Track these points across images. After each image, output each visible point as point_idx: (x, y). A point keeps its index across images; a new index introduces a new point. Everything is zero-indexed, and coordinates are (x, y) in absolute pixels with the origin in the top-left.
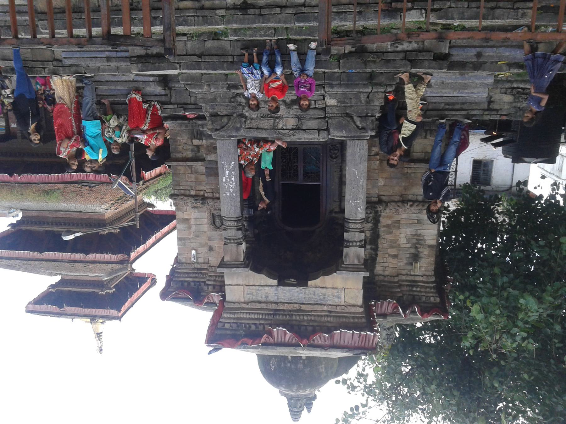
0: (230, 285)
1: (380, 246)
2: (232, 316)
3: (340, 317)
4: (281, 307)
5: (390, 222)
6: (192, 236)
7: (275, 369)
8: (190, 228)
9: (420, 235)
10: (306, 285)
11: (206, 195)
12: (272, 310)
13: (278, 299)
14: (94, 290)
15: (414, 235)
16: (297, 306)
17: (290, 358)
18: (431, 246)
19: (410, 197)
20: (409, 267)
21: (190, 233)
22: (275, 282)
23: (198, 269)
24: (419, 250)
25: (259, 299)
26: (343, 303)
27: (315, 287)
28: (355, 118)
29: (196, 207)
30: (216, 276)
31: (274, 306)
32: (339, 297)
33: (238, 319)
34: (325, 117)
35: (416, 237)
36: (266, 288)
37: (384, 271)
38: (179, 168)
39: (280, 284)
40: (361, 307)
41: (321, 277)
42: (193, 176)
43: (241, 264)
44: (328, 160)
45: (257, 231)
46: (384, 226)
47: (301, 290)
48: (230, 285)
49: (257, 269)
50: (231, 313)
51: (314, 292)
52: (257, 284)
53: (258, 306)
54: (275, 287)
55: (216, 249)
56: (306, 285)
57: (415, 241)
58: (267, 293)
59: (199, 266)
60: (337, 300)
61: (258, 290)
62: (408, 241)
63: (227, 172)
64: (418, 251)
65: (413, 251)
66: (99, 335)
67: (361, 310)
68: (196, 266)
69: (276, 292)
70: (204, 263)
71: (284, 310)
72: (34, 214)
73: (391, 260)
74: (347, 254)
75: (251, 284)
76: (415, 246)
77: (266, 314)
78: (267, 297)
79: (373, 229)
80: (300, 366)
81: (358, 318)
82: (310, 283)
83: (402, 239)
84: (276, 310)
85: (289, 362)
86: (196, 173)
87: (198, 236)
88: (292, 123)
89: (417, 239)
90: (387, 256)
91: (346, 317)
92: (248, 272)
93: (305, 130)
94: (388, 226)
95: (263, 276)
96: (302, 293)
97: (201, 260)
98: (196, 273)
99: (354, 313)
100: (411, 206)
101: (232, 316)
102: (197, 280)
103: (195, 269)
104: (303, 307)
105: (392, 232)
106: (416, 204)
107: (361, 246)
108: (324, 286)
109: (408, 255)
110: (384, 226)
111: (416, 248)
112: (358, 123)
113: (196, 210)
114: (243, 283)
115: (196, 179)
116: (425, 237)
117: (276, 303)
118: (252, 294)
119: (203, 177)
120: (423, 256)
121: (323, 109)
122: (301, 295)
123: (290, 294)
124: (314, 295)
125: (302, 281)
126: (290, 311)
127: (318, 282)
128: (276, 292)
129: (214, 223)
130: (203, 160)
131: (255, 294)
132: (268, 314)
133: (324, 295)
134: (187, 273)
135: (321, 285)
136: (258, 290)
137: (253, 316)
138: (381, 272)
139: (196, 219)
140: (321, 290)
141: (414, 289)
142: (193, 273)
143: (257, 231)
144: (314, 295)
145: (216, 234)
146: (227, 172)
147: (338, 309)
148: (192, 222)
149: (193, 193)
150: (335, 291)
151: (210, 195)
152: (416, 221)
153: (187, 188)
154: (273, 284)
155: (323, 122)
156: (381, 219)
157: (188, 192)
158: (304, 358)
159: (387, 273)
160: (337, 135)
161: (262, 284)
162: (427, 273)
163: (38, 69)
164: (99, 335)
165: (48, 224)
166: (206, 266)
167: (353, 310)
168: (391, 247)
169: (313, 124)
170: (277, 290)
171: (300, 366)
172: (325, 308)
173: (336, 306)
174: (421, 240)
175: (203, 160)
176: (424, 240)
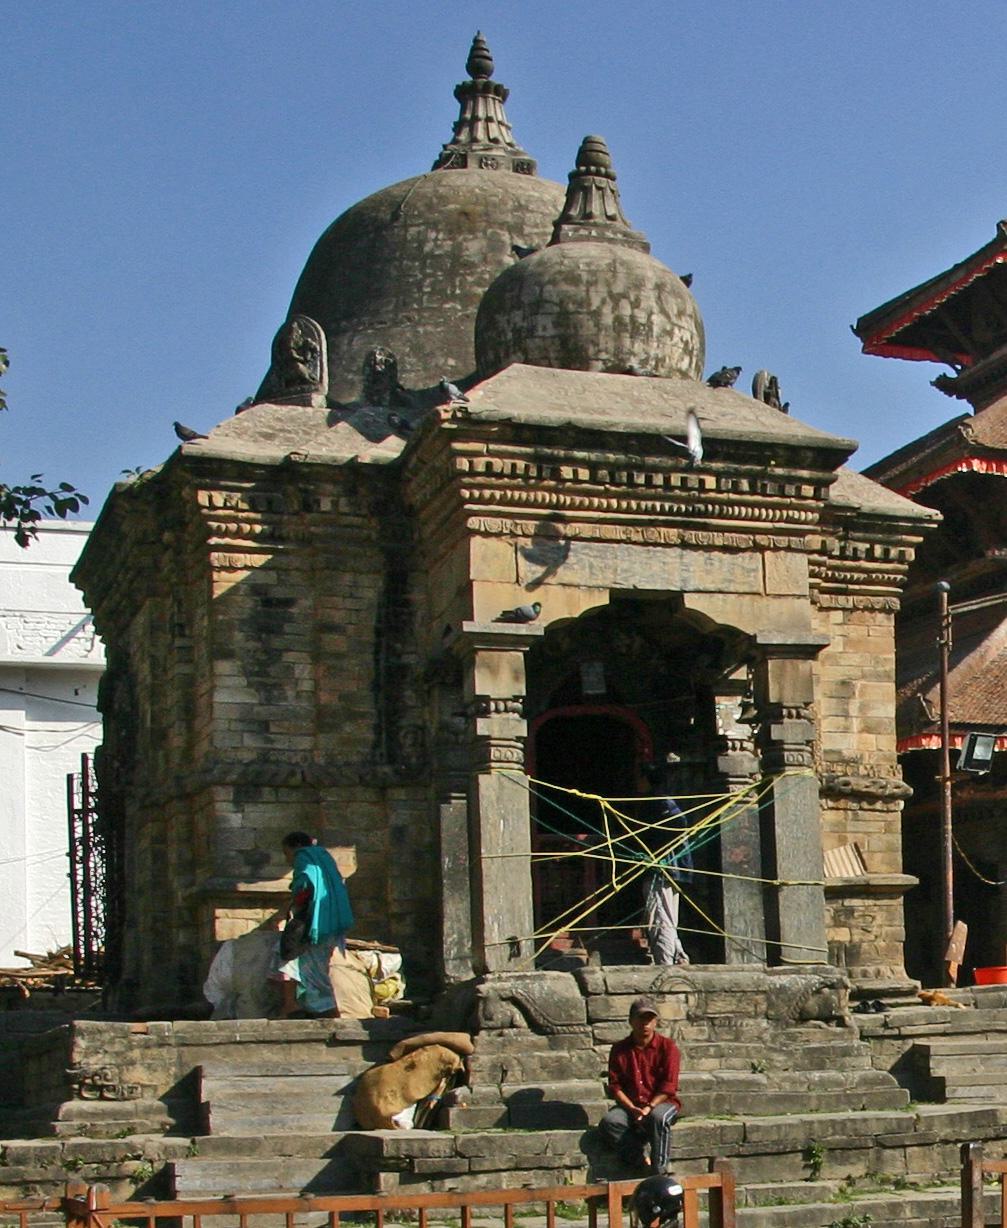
0: (799, 597)
1: (369, 657)
5: (348, 728)
10: (615, 594)
13: (681, 557)
19: (294, 796)
22: (691, 602)
24: (258, 645)
31: (692, 536)
35: (271, 681)
36: (712, 587)
39: (676, 597)
41: (576, 615)
43: (773, 653)
46: (363, 716)
47: (626, 579)
48: (799, 597)
50: (797, 522)
51: (592, 573)
52: (733, 596)
54: (691, 588)
57: (273, 670)
58: (708, 572)
61: (730, 581)
62: (289, 668)
64: (259, 639)
65: (277, 643)
67: (473, 523)
69: (685, 575)
73: (338, 617)
74: (516, 678)
75: (748, 597)
76: (273, 655)
77: (712, 516)
81: (481, 501)
83: (306, 675)
89: (268, 676)
90: (351, 629)
94: (352, 716)
95: (719, 620)
96: (626, 571)
105: (340, 698)
108: (568, 590)
109: (287, 628)
110: (363, 716)
114: (765, 601)
116: (243, 681)
122: (625, 565)
124: (591, 566)
128: (685, 575)
131: (738, 571)
136: (730, 581)
140: (576, 580)
144: (591, 566)
152: (273, 729)
154: (696, 596)
156: (370, 736)
159: (348, 578)
161: (721, 596)
167: (494, 524)
168: (339, 656)
170: (684, 580)
174: (258, 674)
176: (247, 673)
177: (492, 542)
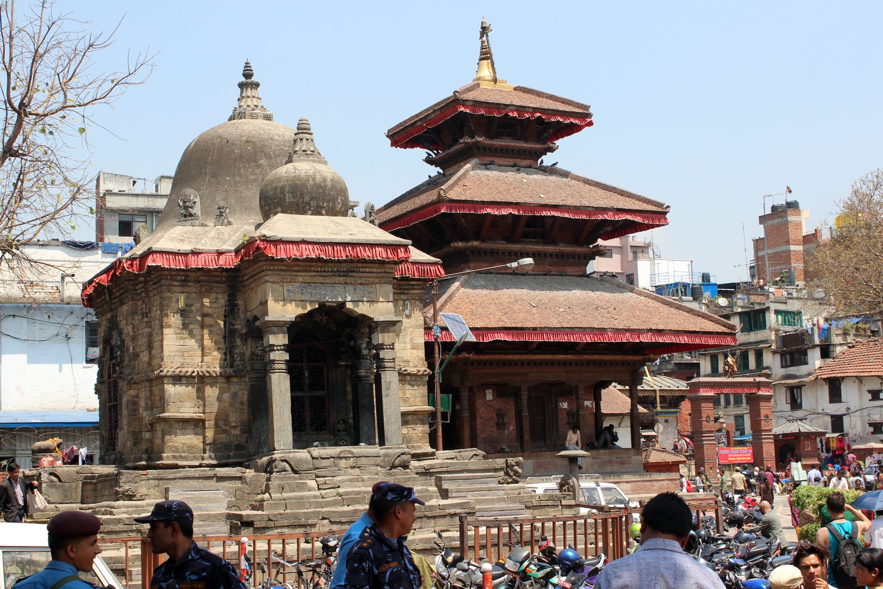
8: (412, 339)
14: (491, 142)
16: (328, 281)
17: (324, 212)
18: (169, 326)
20: (190, 302)
23: (403, 294)
25: (361, 287)
26: (285, 284)
31: (348, 280)
32: (288, 290)
37: (217, 298)
45: (352, 343)
53: (363, 280)
59: (402, 297)
60: (291, 288)
66: (486, 55)
71: (339, 276)
72: (569, 270)
78: (355, 290)
79: (233, 347)
80: (313, 203)
84: (346, 276)
100: (193, 372)
106: (188, 374)
107: (273, 345)
117: (346, 283)
118: (369, 292)
121: (317, 476)
123: (333, 295)
133: (302, 293)
137: (368, 270)
138: (220, 296)
140: (306, 299)
143: (352, 343)
148: (409, 346)
150: (292, 298)
158: (310, 212)
162: (169, 294)
164: (486, 55)
165: (551, 255)
167: (275, 279)
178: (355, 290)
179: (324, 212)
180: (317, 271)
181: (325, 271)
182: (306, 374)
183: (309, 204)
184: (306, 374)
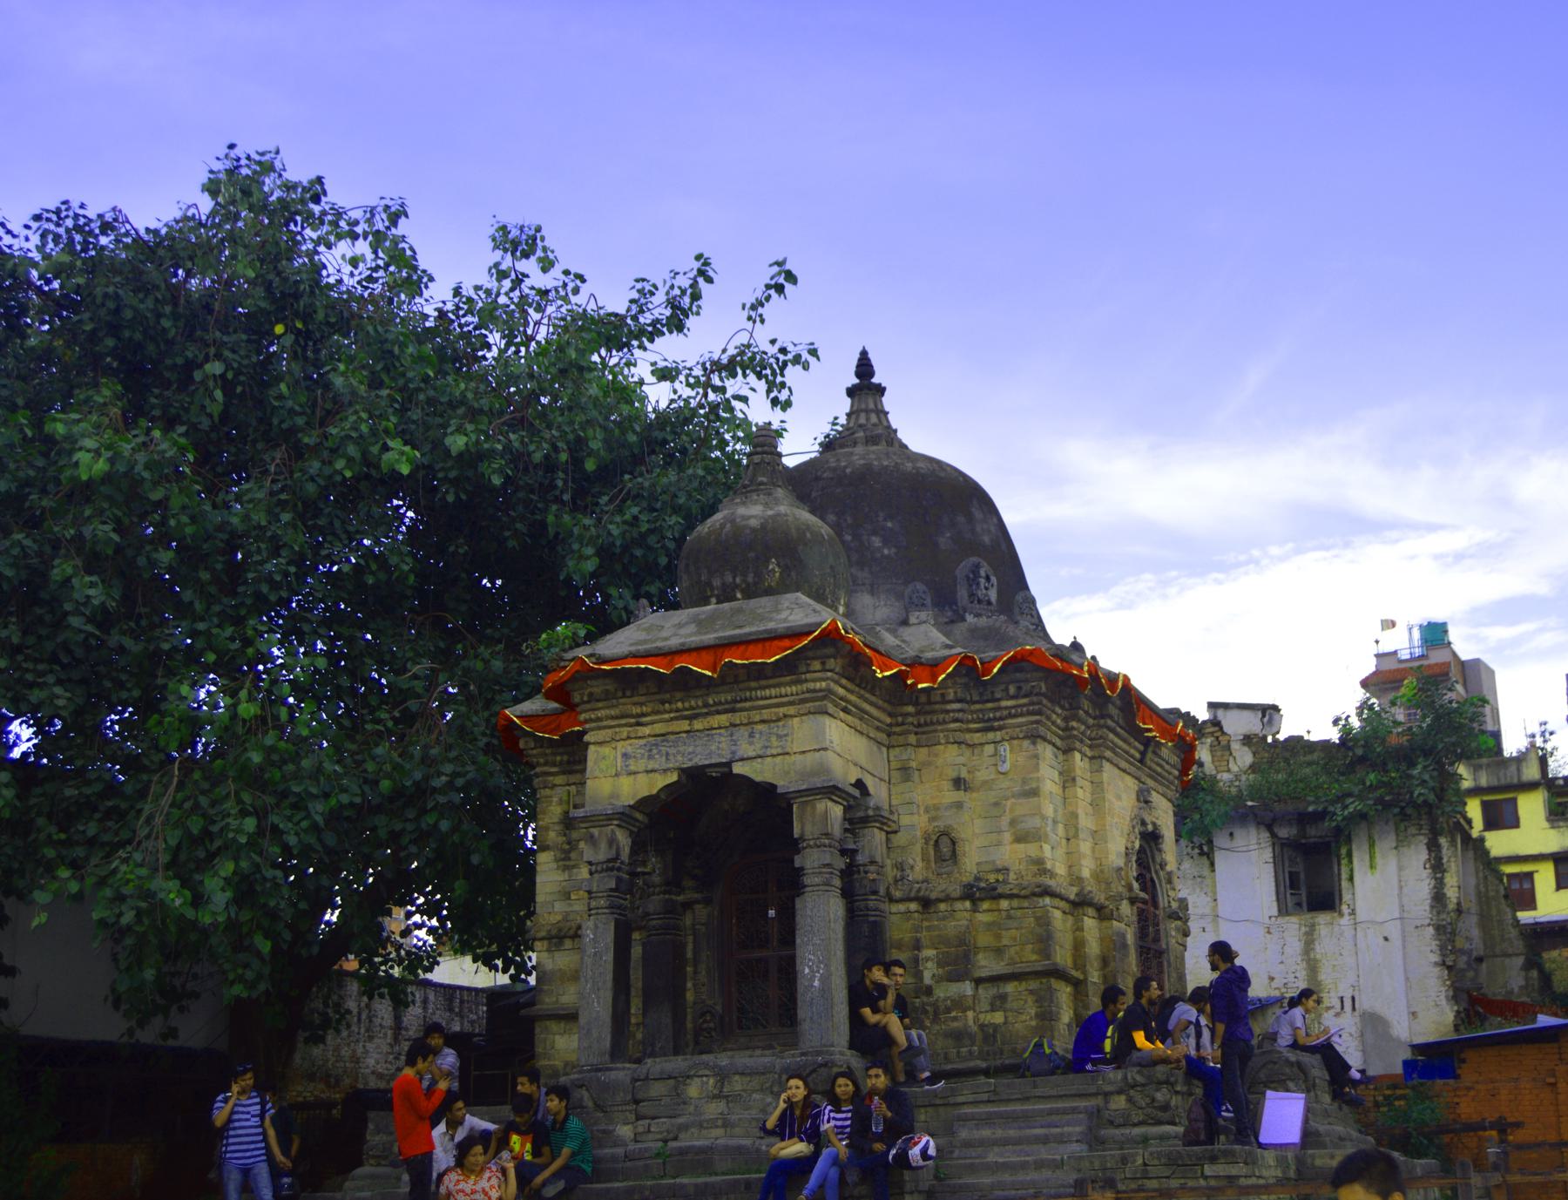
2: (811, 685)
3: (622, 717)
4: (723, 719)
6: (1009, 803)
7: (768, 561)
8: (1013, 823)
9: (566, 868)
11: (968, 904)
12: (742, 710)
15: (574, 867)
16: (698, 725)
17: (739, 595)
21: (1012, 810)
22: (738, 769)
27: (665, 771)
28: (590, 1104)
29: (998, 871)
30: (944, 722)
33: (801, 682)
34: (637, 1102)
38: (1034, 957)
40: (588, 744)
42: (1005, 942)
44: (719, 1008)
49: (766, 792)
50: (815, 691)
53: (766, 714)
55: (947, 785)
56: (683, 771)
57: (573, 855)
58: (751, 743)
59: (991, 735)
60: (630, 750)
63: (816, 983)
68: (999, 735)
70: (982, 744)
71: (718, 713)
76: (572, 845)
78: (751, 735)
81: (591, 720)
82: (673, 777)
84: (733, 711)
85: (737, 586)
86: (999, 951)
87: (996, 804)
88: (693, 1090)
91: (613, 718)
92: (783, 785)
93: (670, 1078)
97: (989, 749)
98: (995, 719)
99: (600, 728)
101: (811, 685)
102: (990, 705)
103: (1000, 728)
104: (685, 725)
111: (569, 843)
112: (586, 1094)
113: (999, 864)
115: (998, 937)
118: (779, 737)
119: (984, 939)
120: (557, 827)
125: (693, 775)
126: (707, 714)
127: (661, 781)
129: (954, 843)
130: (978, 982)
131: (774, 739)
132: (746, 700)
133: (650, 757)
134: (1011, 716)
135: (657, 775)
137: (773, 692)
139: (999, 844)
141: (565, 758)
142: (1001, 719)
145: (948, 819)
146: (816, 983)
147: (625, 731)
148: (1007, 837)
149: (1004, 904)
151: (959, 905)
153: (1019, 913)
155: (640, 1096)
157: (1015, 903)
160: (621, 1073)
162: (548, 792)
163: (1156, 1162)
166: (977, 738)
169: (657, 1089)
171: (717, 582)
172: (647, 730)
173: (629, 738)
175: (978, 982)
176: (557, 860)
177: (606, 750)
178: (751, 735)
179: (739, 595)
180: (677, 710)
181: (692, 708)
182: (772, 913)
183: (709, 584)
184: (772, 913)
